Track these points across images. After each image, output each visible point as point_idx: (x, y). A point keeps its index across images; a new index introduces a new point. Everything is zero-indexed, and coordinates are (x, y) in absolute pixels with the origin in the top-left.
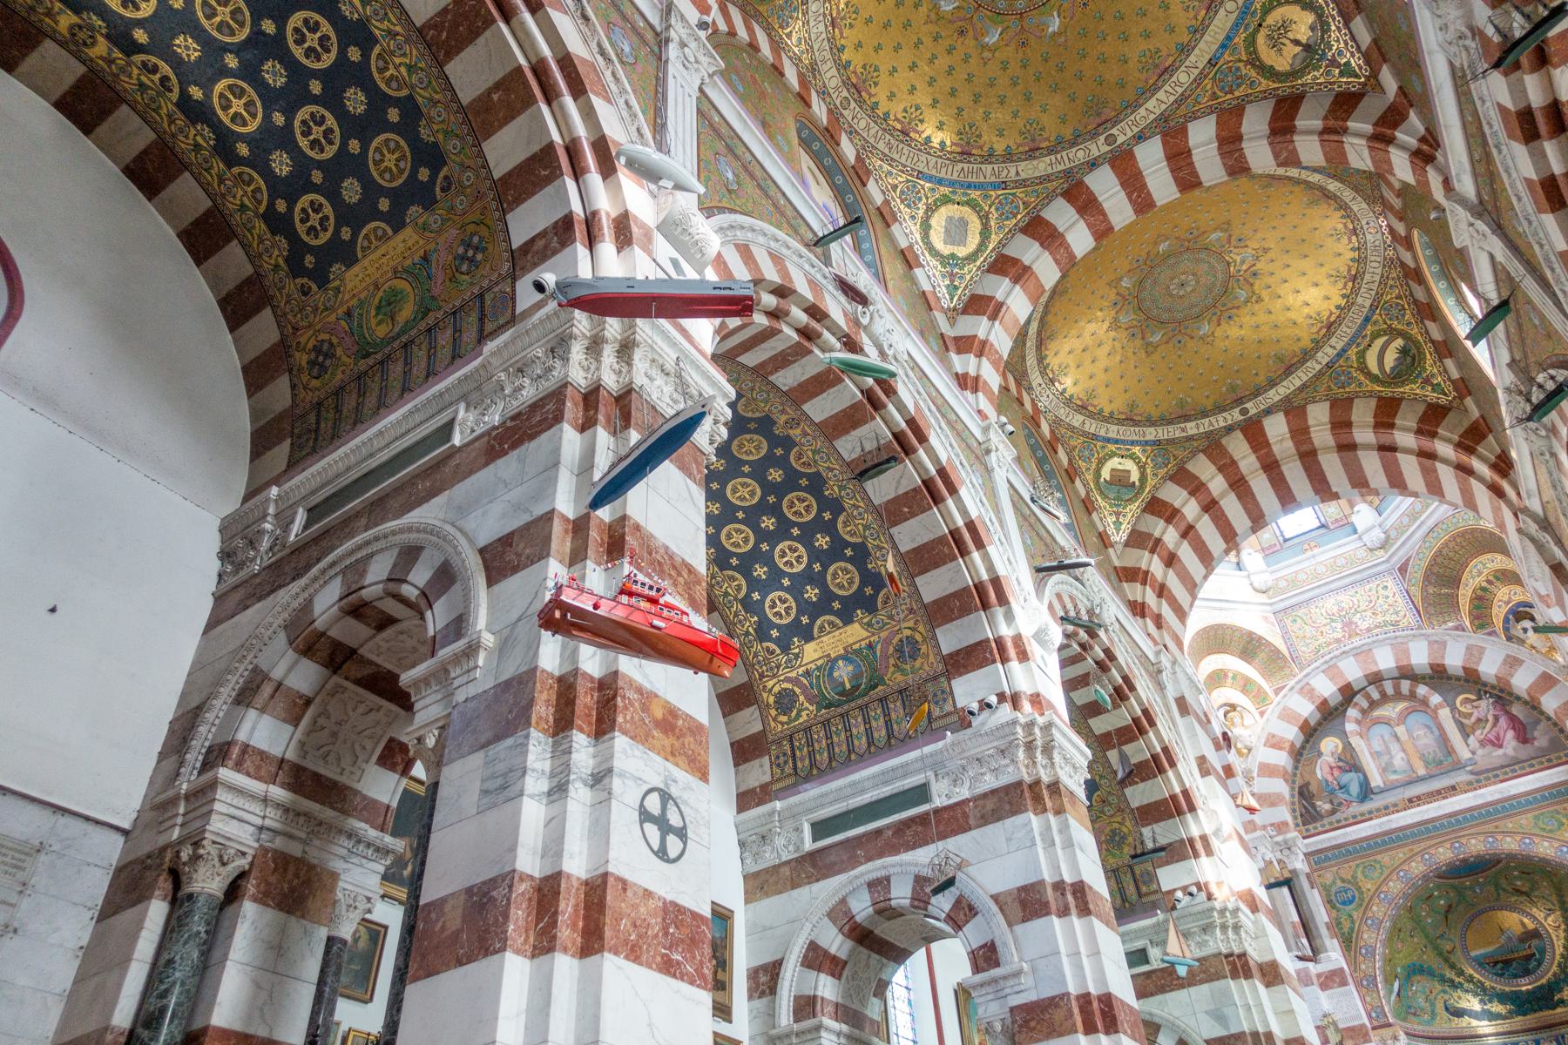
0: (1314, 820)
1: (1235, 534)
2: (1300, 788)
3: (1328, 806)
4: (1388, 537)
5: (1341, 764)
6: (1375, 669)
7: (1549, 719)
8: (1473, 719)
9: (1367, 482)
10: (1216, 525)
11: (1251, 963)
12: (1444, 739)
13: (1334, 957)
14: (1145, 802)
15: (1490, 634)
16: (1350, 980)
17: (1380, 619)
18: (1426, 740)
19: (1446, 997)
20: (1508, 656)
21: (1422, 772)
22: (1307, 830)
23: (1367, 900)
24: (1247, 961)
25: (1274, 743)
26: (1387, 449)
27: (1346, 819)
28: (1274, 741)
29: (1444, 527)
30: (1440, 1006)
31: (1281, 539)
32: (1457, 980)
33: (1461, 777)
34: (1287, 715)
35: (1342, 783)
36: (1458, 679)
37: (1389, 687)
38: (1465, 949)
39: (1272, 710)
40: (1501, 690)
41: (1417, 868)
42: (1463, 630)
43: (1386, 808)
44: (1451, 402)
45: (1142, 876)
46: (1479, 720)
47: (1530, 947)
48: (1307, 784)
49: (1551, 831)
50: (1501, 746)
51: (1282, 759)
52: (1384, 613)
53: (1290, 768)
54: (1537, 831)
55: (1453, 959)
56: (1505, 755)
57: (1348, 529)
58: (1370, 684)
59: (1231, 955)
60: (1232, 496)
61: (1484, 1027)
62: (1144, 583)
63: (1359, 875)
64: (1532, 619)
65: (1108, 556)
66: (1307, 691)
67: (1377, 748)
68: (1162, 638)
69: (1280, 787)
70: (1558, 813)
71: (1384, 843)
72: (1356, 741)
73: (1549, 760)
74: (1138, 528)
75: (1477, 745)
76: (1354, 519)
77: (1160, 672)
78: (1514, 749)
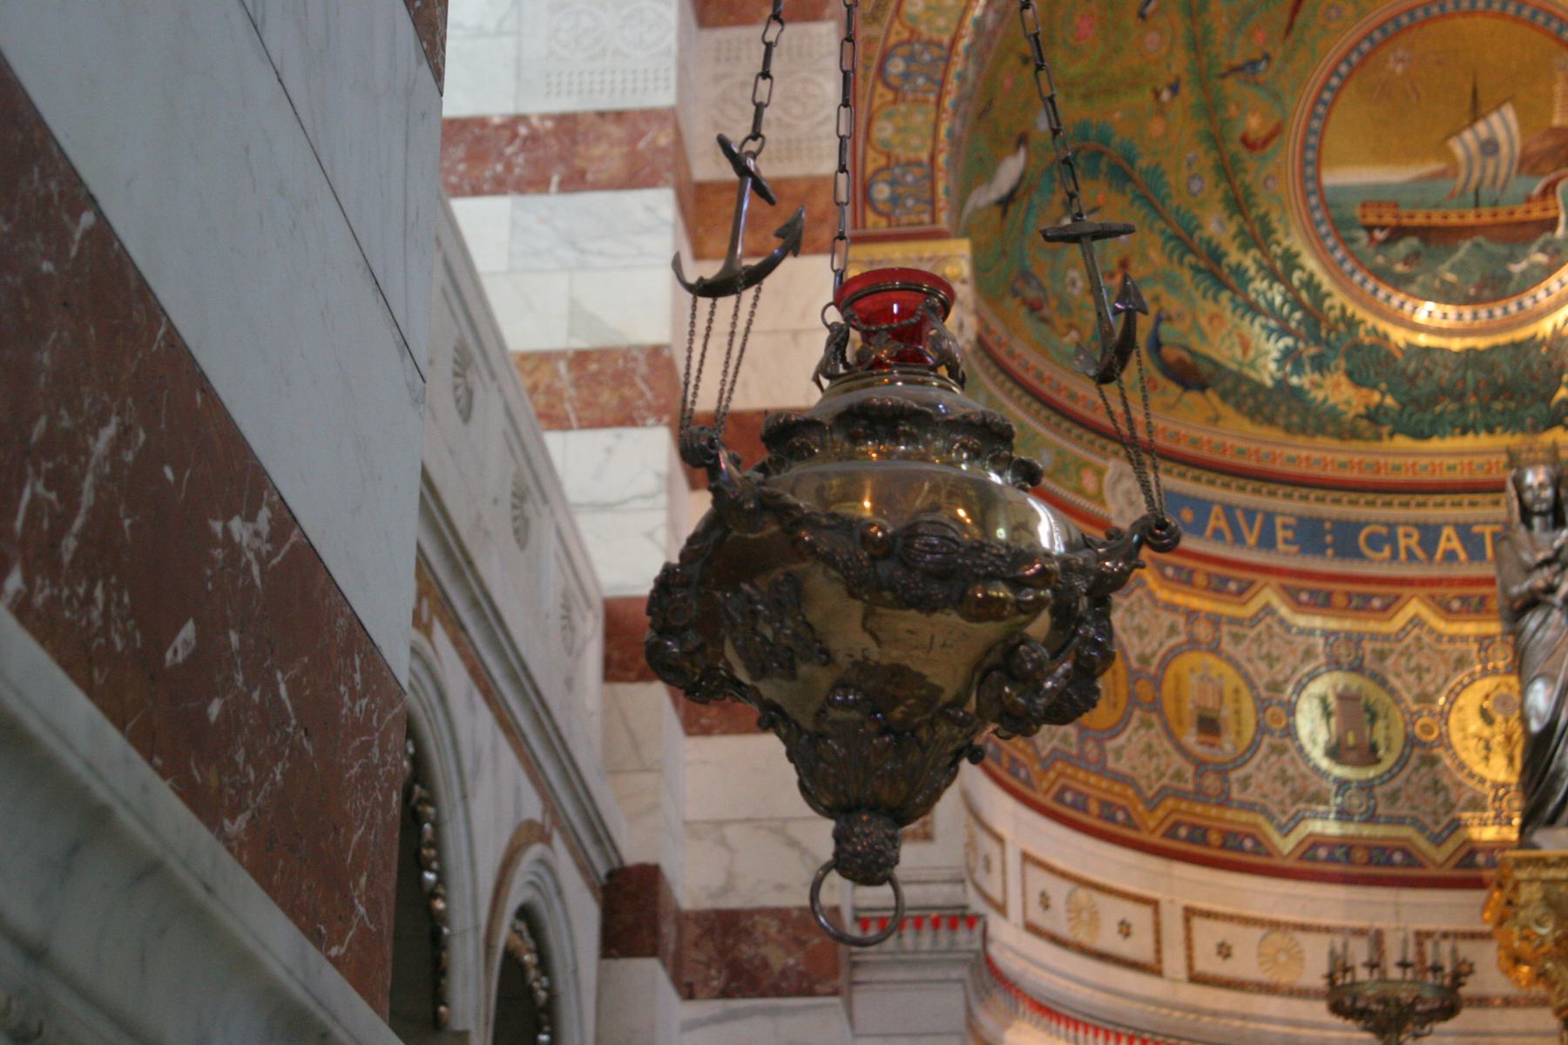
32: (1234, 256)
47: (1549, 190)
55: (1254, 171)
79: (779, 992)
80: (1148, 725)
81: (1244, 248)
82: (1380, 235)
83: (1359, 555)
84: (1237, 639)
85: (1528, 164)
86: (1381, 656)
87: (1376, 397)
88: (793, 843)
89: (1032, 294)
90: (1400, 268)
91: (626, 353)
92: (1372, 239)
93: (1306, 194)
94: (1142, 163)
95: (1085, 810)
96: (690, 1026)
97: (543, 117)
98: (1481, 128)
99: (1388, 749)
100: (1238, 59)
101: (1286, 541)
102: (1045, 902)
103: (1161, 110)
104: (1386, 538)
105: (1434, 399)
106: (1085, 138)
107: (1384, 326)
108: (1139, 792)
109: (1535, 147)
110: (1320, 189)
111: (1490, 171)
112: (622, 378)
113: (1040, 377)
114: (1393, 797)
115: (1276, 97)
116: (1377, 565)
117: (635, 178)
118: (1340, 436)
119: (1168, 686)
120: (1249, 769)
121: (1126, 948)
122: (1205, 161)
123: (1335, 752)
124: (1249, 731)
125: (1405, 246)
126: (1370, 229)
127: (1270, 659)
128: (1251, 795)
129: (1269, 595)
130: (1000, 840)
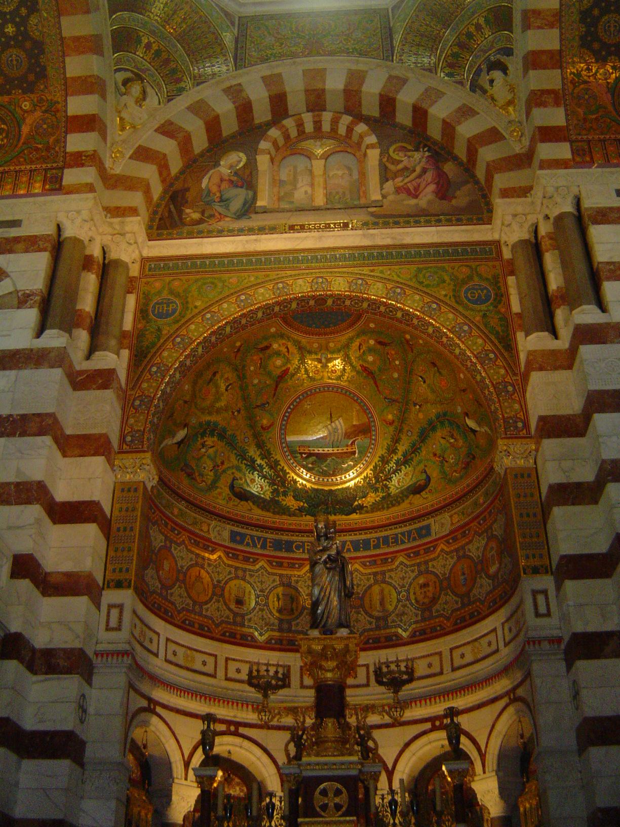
0: (174, 225)
3: (196, 216)
5: (234, 178)
6: (319, 86)
7: (477, 182)
8: (400, 166)
22: (158, 235)
23: (188, 316)
25: (167, 130)
32: (259, 461)
35: (225, 196)
36: (403, 127)
37: (327, 117)
38: (284, 431)
39: (182, 103)
41: (264, 295)
46: (406, 168)
47: (353, 443)
48: (188, 190)
49: (427, 286)
50: (416, 197)
56: (417, 205)
58: (308, 111)
64: (505, 70)
66: (235, 92)
70: (443, 269)
71: (240, 263)
72: (263, 161)
78: (430, 203)
79: (61, 673)
80: (218, 601)
81: (262, 459)
82: (304, 455)
83: (293, 552)
84: (251, 576)
85: (347, 435)
86: (297, 582)
87: (302, 504)
88: (70, 629)
90: (310, 466)
92: (302, 456)
93: (282, 443)
94: (229, 433)
95: (194, 627)
96: (34, 683)
97: (17, 415)
98: (333, 424)
99: (297, 610)
100: (259, 404)
101: (270, 547)
102: (175, 654)
103: (234, 418)
104: (301, 546)
105: (318, 505)
106: (209, 425)
108: (213, 621)
109: (349, 430)
111: (336, 437)
113: (190, 495)
114: (297, 625)
115: (272, 415)
116: (298, 555)
117: (40, 434)
118: (290, 516)
119: (227, 589)
120: (252, 615)
121: (204, 669)
123: (280, 611)
124: (253, 604)
126: (301, 454)
127: (262, 582)
130: (158, 634)
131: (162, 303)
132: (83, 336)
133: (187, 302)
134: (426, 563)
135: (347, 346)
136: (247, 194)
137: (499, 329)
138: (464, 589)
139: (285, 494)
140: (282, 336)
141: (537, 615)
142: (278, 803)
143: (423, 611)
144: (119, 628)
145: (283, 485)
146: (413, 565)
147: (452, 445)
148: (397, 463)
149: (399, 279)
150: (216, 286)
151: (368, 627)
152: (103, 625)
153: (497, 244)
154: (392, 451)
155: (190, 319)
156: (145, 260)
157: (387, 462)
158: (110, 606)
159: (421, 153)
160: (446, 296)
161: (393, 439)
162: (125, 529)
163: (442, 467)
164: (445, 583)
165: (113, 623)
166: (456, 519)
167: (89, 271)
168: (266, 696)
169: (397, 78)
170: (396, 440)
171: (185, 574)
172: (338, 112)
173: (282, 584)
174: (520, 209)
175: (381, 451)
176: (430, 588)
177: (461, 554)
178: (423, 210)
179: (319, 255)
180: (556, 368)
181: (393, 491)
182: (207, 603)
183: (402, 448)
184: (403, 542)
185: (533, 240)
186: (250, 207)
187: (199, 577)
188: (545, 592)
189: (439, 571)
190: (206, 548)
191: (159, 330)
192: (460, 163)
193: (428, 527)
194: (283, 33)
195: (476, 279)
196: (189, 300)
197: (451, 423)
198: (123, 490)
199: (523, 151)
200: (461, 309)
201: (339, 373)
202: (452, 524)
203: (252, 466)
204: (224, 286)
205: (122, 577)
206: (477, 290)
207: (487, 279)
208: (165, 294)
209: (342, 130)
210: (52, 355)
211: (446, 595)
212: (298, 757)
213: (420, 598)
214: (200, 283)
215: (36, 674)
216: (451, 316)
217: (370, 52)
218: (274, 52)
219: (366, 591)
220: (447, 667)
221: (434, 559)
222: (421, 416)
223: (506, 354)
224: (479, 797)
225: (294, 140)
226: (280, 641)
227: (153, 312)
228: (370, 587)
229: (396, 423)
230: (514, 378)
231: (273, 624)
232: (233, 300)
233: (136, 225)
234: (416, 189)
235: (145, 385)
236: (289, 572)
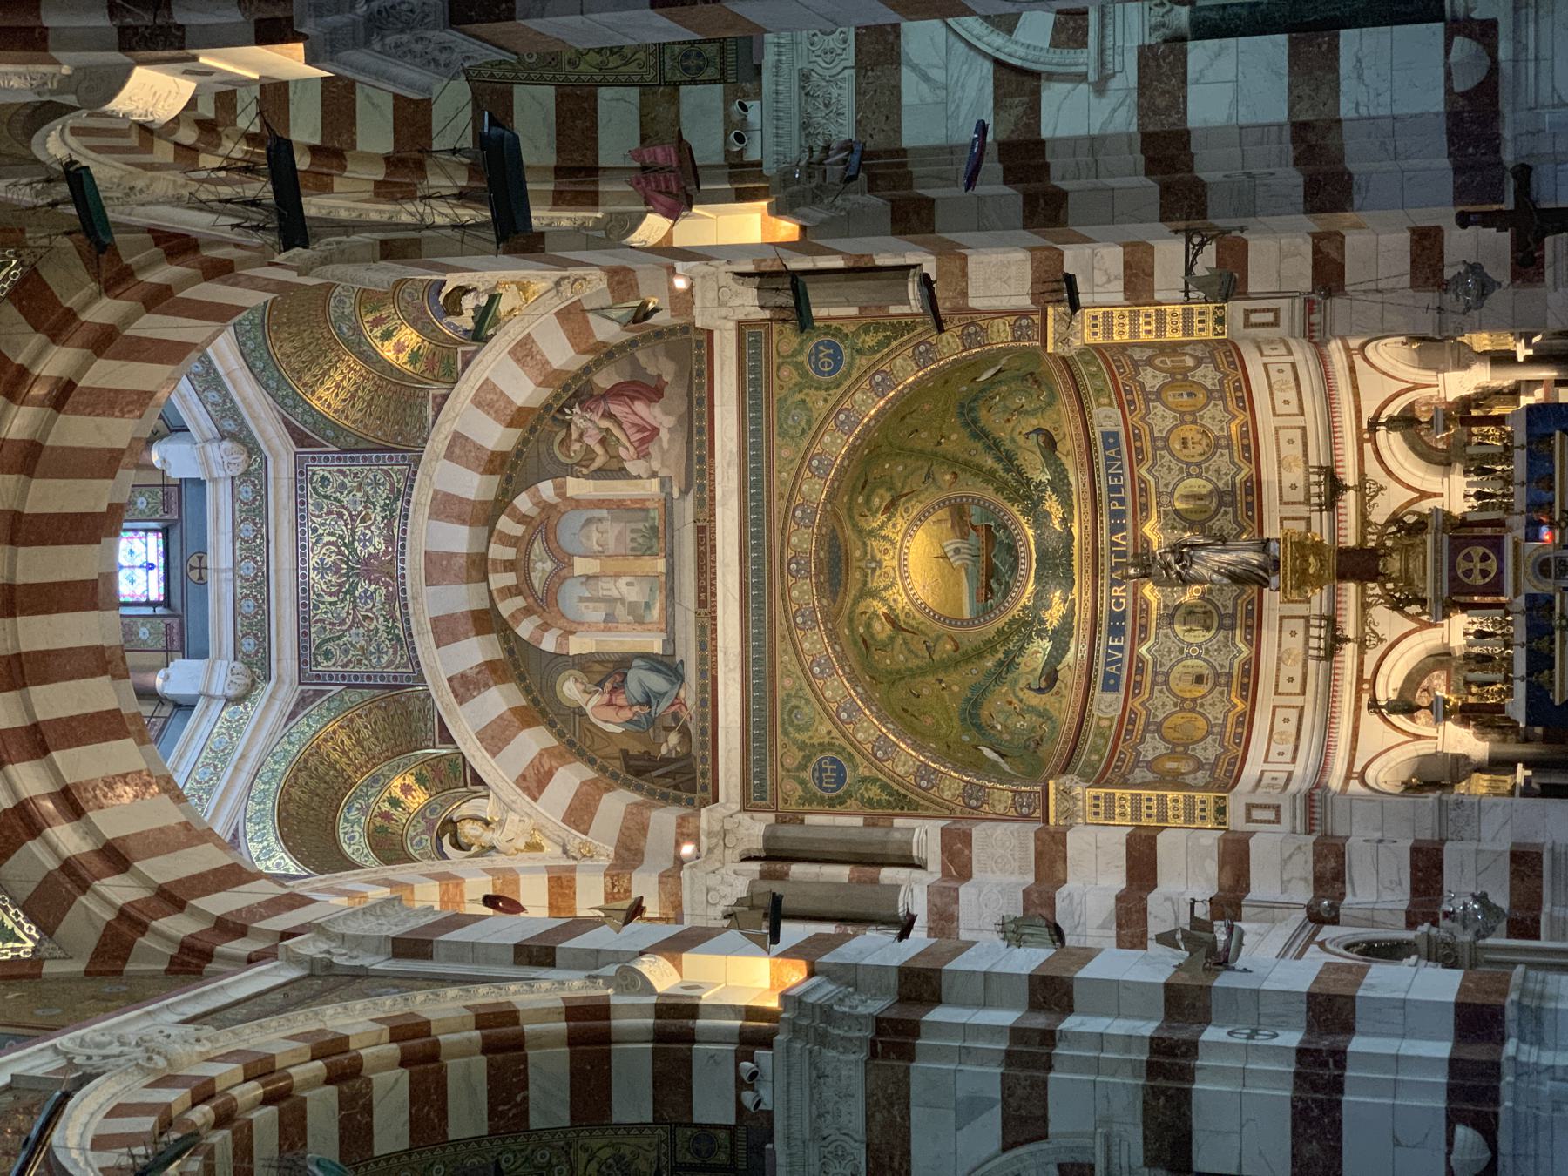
1: (115, 713)
2: (628, 768)
3: (674, 738)
4: (233, 437)
5: (608, 685)
6: (462, 561)
7: (633, 343)
8: (598, 449)
9: (111, 450)
10: (79, 742)
11: (893, 1014)
12: (617, 507)
13: (925, 836)
14: (567, 1095)
15: (466, 364)
16: (963, 826)
17: (377, 514)
18: (610, 533)
19: (1022, 683)
20: (512, 353)
21: (660, 566)
22: (704, 788)
23: (843, 742)
24: (889, 1020)
25: (535, 782)
26: (63, 395)
27: (703, 717)
28: (533, 785)
29: (251, 345)
30: (1035, 700)
31: (159, 610)
32: (1001, 655)
33: (687, 510)
34: (495, 738)
35: (639, 696)
36: (524, 441)
37: (497, 552)
40: (566, 388)
41: (815, 643)
42: (446, 397)
43: (702, 646)
44: (21, 264)
45: (698, 1153)
46: (602, 442)
47: (975, 528)
48: (625, 753)
49: (809, 423)
50: (656, 431)
51: (569, 779)
52: (368, 500)
53: (590, 773)
54: (806, 444)
55: (966, 646)
57: (190, 491)
58: (486, 579)
59: (873, 1043)
60: (37, 692)
61: (1076, 652)
62: (142, 928)
63: (801, 737)
64: (463, 291)
65: (58, 979)
66: (464, 687)
67: (596, 614)
68: (264, 933)
69: (615, 804)
72: (579, 645)
73: (700, 374)
74: (23, 896)
75: (642, 463)
76: (175, 474)
77: (330, 965)
78: (666, 413)
80: (1202, 705)
81: (997, 651)
84: (1162, 665)
88: (1290, 857)
89: (1033, 745)
91: (1118, 910)
96: (1354, 895)
102: (1281, 754)
103: (948, 687)
107: (1027, 595)
110: (973, 620)
112: (1128, 911)
114: (1225, 607)
121: (1294, 721)
122: (964, 670)
123: (1208, 629)
124: (1200, 662)
125: (995, 586)
127: (1170, 652)
128: (1227, 664)
129: (1143, 650)
131: (821, 780)
132: (887, 874)
133: (821, 744)
134: (1154, 440)
135: (860, 532)
136: (639, 667)
137: (881, 336)
138: (1201, 396)
139: (1043, 622)
140: (851, 620)
141: (1276, 323)
142: (1476, 627)
143: (1217, 446)
144: (1277, 808)
145: (1031, 623)
146: (1154, 456)
147: (1003, 398)
148: (1007, 471)
149: (798, 461)
150: (797, 707)
151: (1230, 516)
152: (1275, 827)
153: (743, 326)
154: (989, 476)
155: (848, 740)
156: (744, 809)
157: (1006, 483)
158: (1249, 819)
159: (575, 419)
160: (826, 401)
161: (976, 475)
162: (1149, 808)
163: (1027, 412)
164: (1188, 418)
165: (1271, 815)
166: (1105, 400)
167: (787, 874)
168: (1348, 640)
169: (450, 446)
170: (978, 470)
171: (1175, 745)
172: (490, 536)
173: (1171, 623)
174: (712, 295)
175: (988, 493)
176: (1189, 435)
177: (1152, 397)
178: (680, 421)
179: (751, 567)
180: (965, 275)
181: (1046, 477)
182: (1207, 719)
183: (989, 462)
184: (1120, 467)
185: (757, 280)
186: (661, 663)
187: (1175, 729)
188: (1247, 313)
189: (1169, 424)
190: (1132, 722)
191: (863, 780)
192: (598, 363)
193: (1105, 435)
194: (344, 615)
195: (800, 359)
196: (815, 741)
197: (975, 399)
198: (1097, 814)
199: (605, 279)
200: (847, 383)
201: (888, 545)
202: (1111, 405)
203: (1008, 664)
204: (796, 696)
205: (1211, 808)
206: (818, 359)
207: (801, 344)
208: (806, 775)
209: (518, 530)
210: (938, 901)
211: (1202, 417)
212: (1423, 602)
213: (1199, 449)
214: (791, 729)
215: (1343, 895)
216: (858, 396)
217: (392, 485)
218: (381, 628)
219: (1182, 518)
220: (1299, 421)
221: (1152, 431)
222: (954, 437)
223: (920, 329)
224: (1464, 393)
225: (531, 600)
226: (1249, 628)
227: (833, 790)
228: (1176, 511)
229: (957, 470)
230: (956, 322)
231: (1226, 637)
232: (819, 683)
233: (707, 818)
234: (641, 429)
235: (947, 795)
236: (1154, 616)
